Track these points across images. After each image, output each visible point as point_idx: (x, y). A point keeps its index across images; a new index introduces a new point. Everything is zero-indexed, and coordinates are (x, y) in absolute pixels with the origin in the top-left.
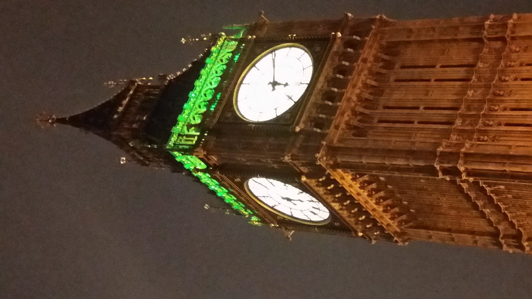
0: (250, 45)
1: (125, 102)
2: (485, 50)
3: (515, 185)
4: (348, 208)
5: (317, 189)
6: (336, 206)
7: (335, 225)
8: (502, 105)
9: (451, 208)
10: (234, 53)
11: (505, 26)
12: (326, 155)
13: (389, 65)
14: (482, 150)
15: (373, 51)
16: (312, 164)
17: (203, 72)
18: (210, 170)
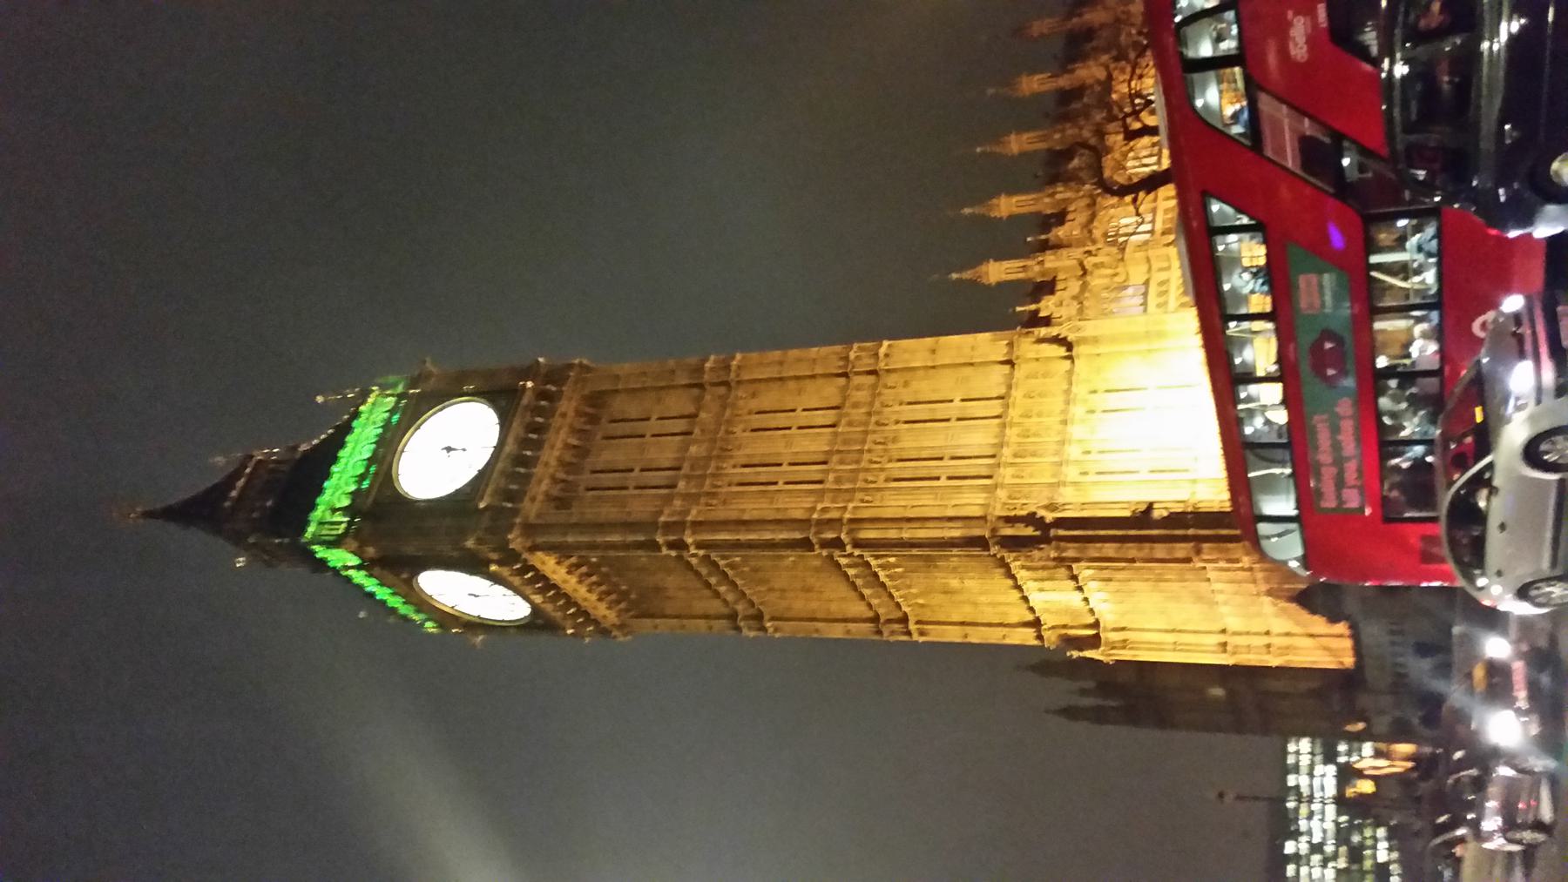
1: (241, 483)
2: (708, 397)
4: (553, 600)
5: (511, 579)
6: (538, 599)
7: (536, 624)
8: (732, 462)
10: (392, 412)
12: (522, 535)
13: (594, 420)
14: (713, 516)
15: (574, 404)
17: (349, 438)
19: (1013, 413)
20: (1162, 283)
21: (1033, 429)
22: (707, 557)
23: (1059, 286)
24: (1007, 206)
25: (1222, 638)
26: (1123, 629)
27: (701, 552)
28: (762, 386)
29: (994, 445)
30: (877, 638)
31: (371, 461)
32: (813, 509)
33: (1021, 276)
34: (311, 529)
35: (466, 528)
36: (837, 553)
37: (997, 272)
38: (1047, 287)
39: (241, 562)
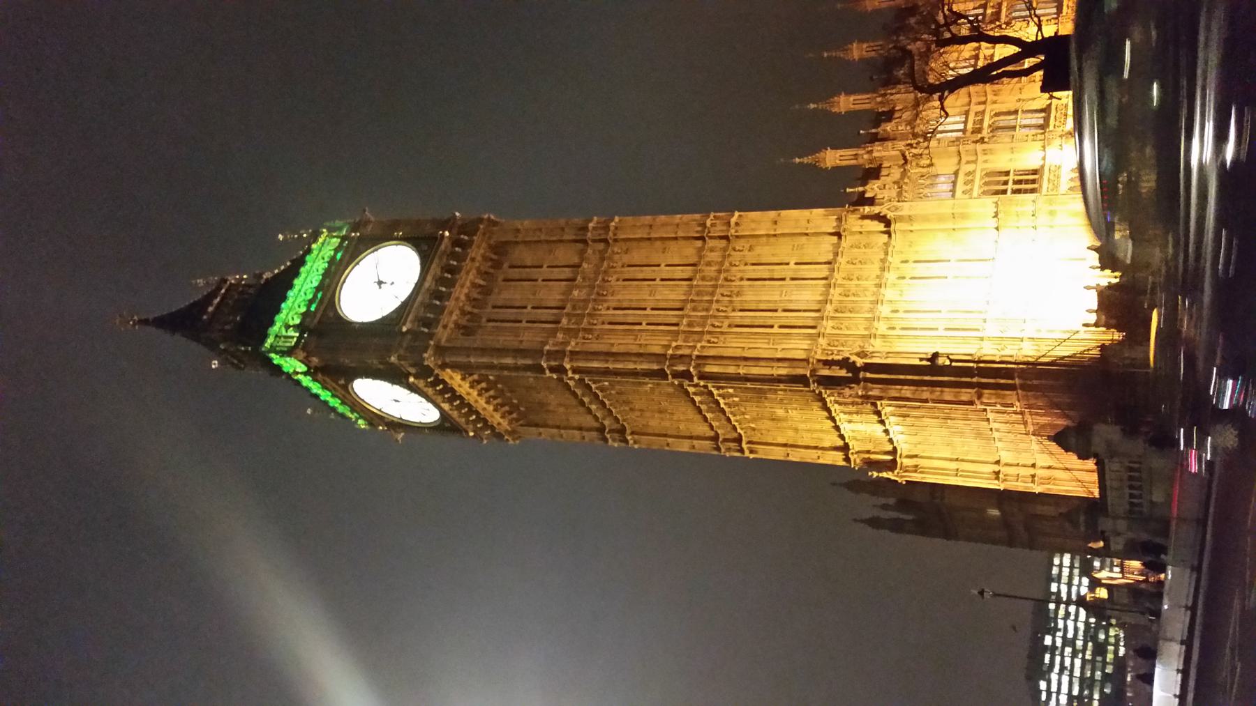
2: (590, 251)
3: (619, 382)
4: (459, 408)
5: (426, 389)
6: (446, 406)
7: (445, 426)
8: (606, 305)
9: (560, 405)
10: (336, 250)
11: (608, 227)
12: (435, 355)
13: (497, 265)
17: (302, 269)
18: (312, 372)
21: (853, 289)
22: (581, 380)
23: (884, 172)
24: (845, 103)
25: (996, 468)
26: (916, 456)
27: (577, 377)
28: (635, 244)
29: (820, 302)
30: (716, 453)
31: (318, 289)
32: (668, 347)
34: (270, 341)
35: (390, 347)
36: (686, 383)
37: (833, 158)
38: (873, 173)
39: (215, 364)
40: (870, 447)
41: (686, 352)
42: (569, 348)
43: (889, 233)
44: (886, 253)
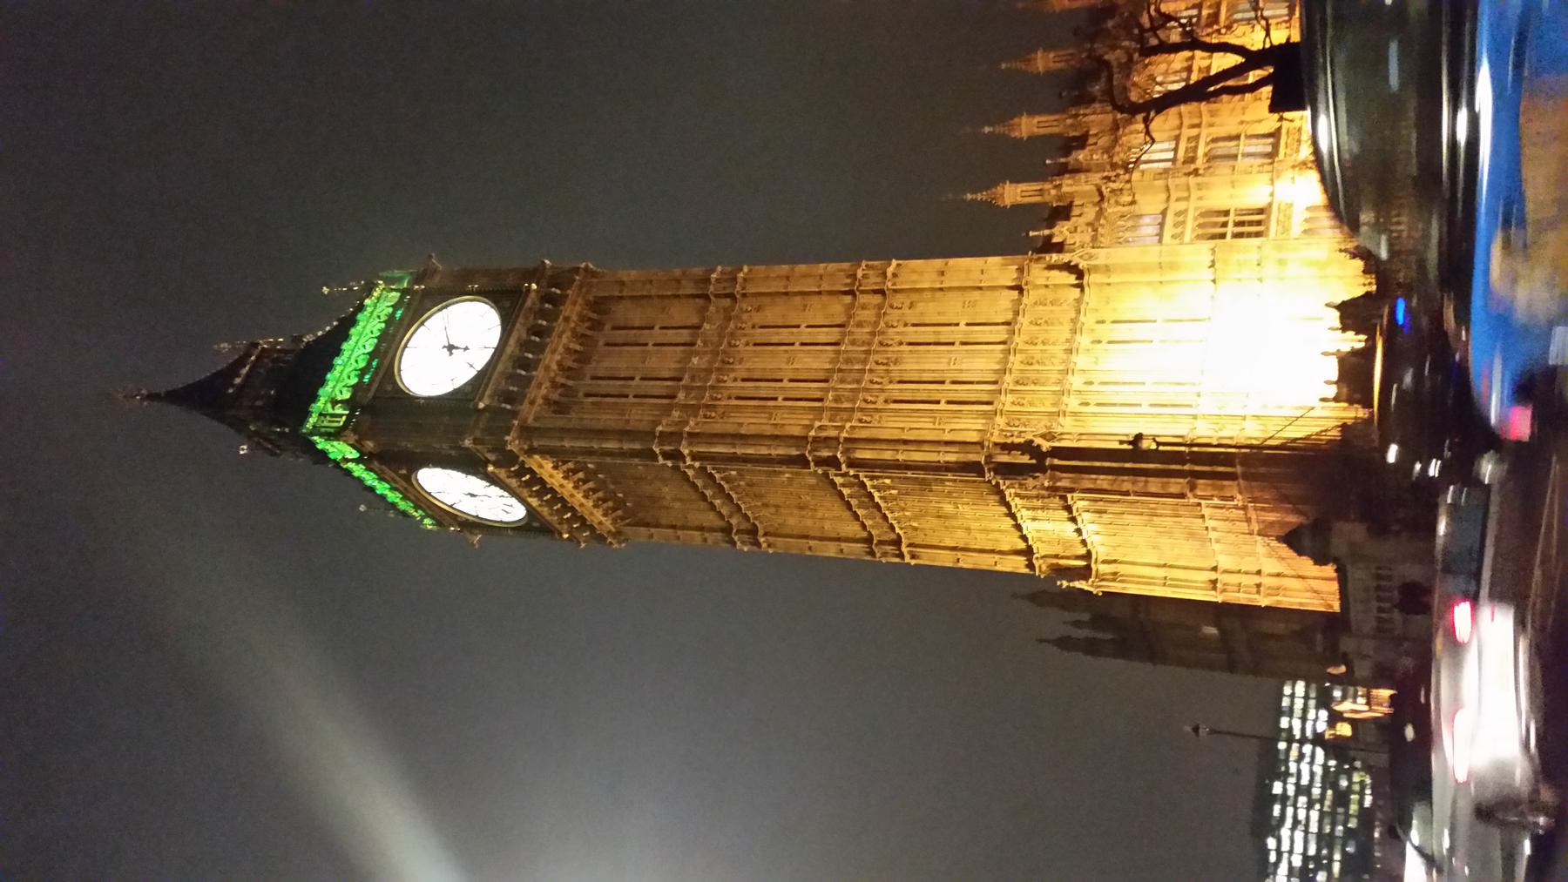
0: (417, 298)
2: (712, 308)
4: (550, 503)
5: (508, 481)
6: (534, 502)
7: (532, 526)
8: (732, 375)
9: (675, 499)
10: (395, 307)
11: (735, 280)
12: (519, 438)
13: (597, 326)
14: (709, 429)
15: (578, 308)
16: (500, 449)
17: (353, 331)
18: (365, 459)
19: (1018, 340)
20: (1178, 214)
21: (1038, 356)
23: (1076, 211)
24: (1028, 126)
25: (1213, 576)
26: (1115, 561)
27: (697, 464)
28: (767, 300)
29: (996, 372)
30: (869, 558)
31: (372, 355)
32: (810, 427)
33: (1038, 199)
34: (312, 420)
35: (464, 427)
36: (832, 472)
37: (1013, 194)
38: (1062, 212)
39: (244, 450)
40: (1059, 550)
41: (833, 433)
42: (687, 429)
43: (1081, 287)
44: (1078, 312)
